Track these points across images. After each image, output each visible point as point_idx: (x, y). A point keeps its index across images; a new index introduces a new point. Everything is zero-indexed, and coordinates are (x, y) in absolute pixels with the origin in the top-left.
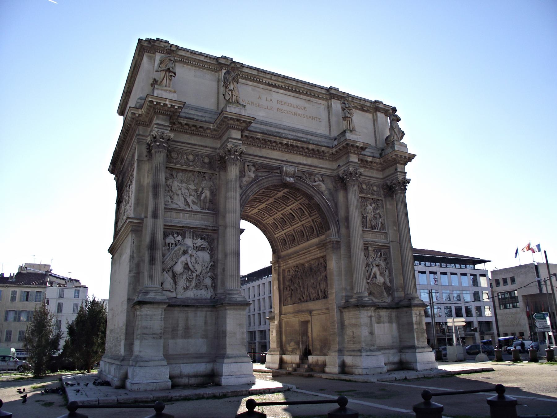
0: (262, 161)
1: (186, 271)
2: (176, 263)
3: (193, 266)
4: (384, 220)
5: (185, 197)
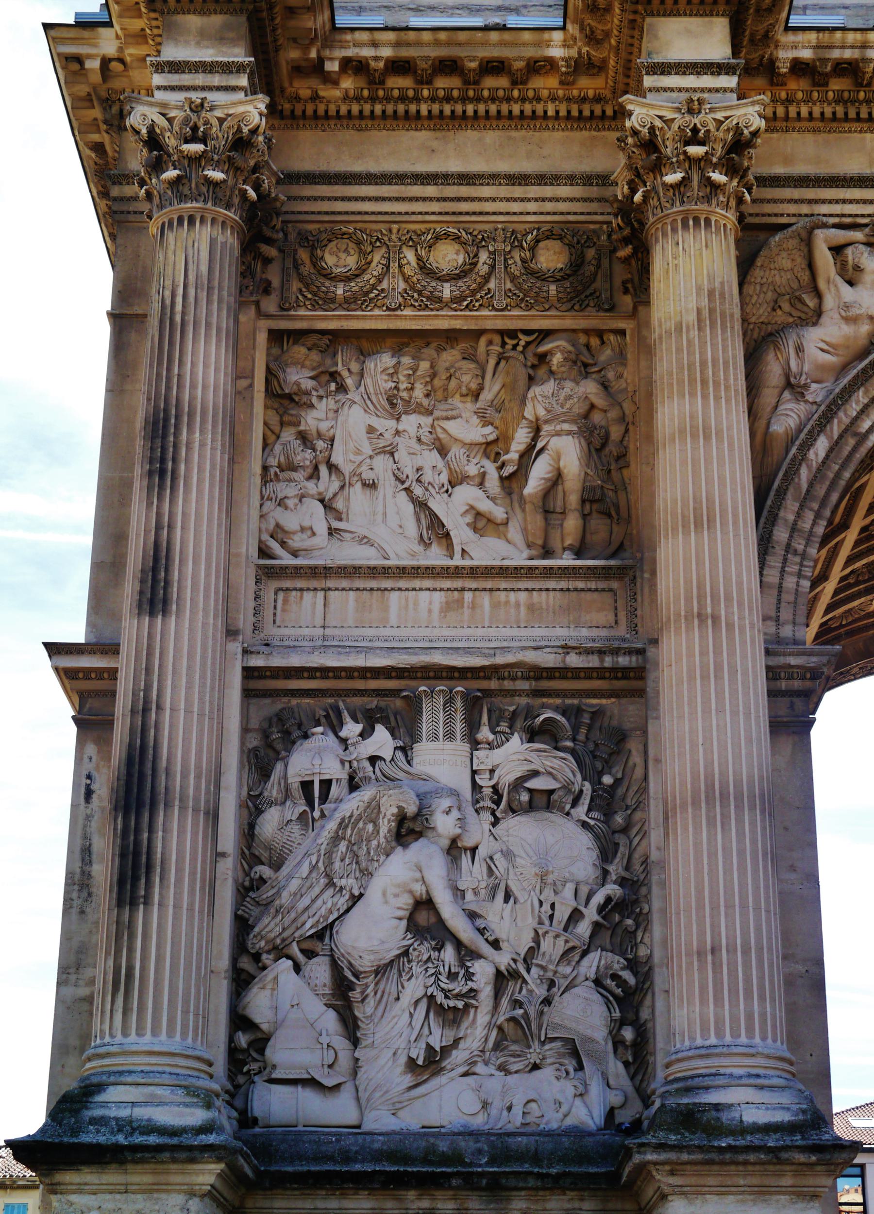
1: (424, 950)
2: (356, 899)
3: (472, 916)
5: (418, 491)
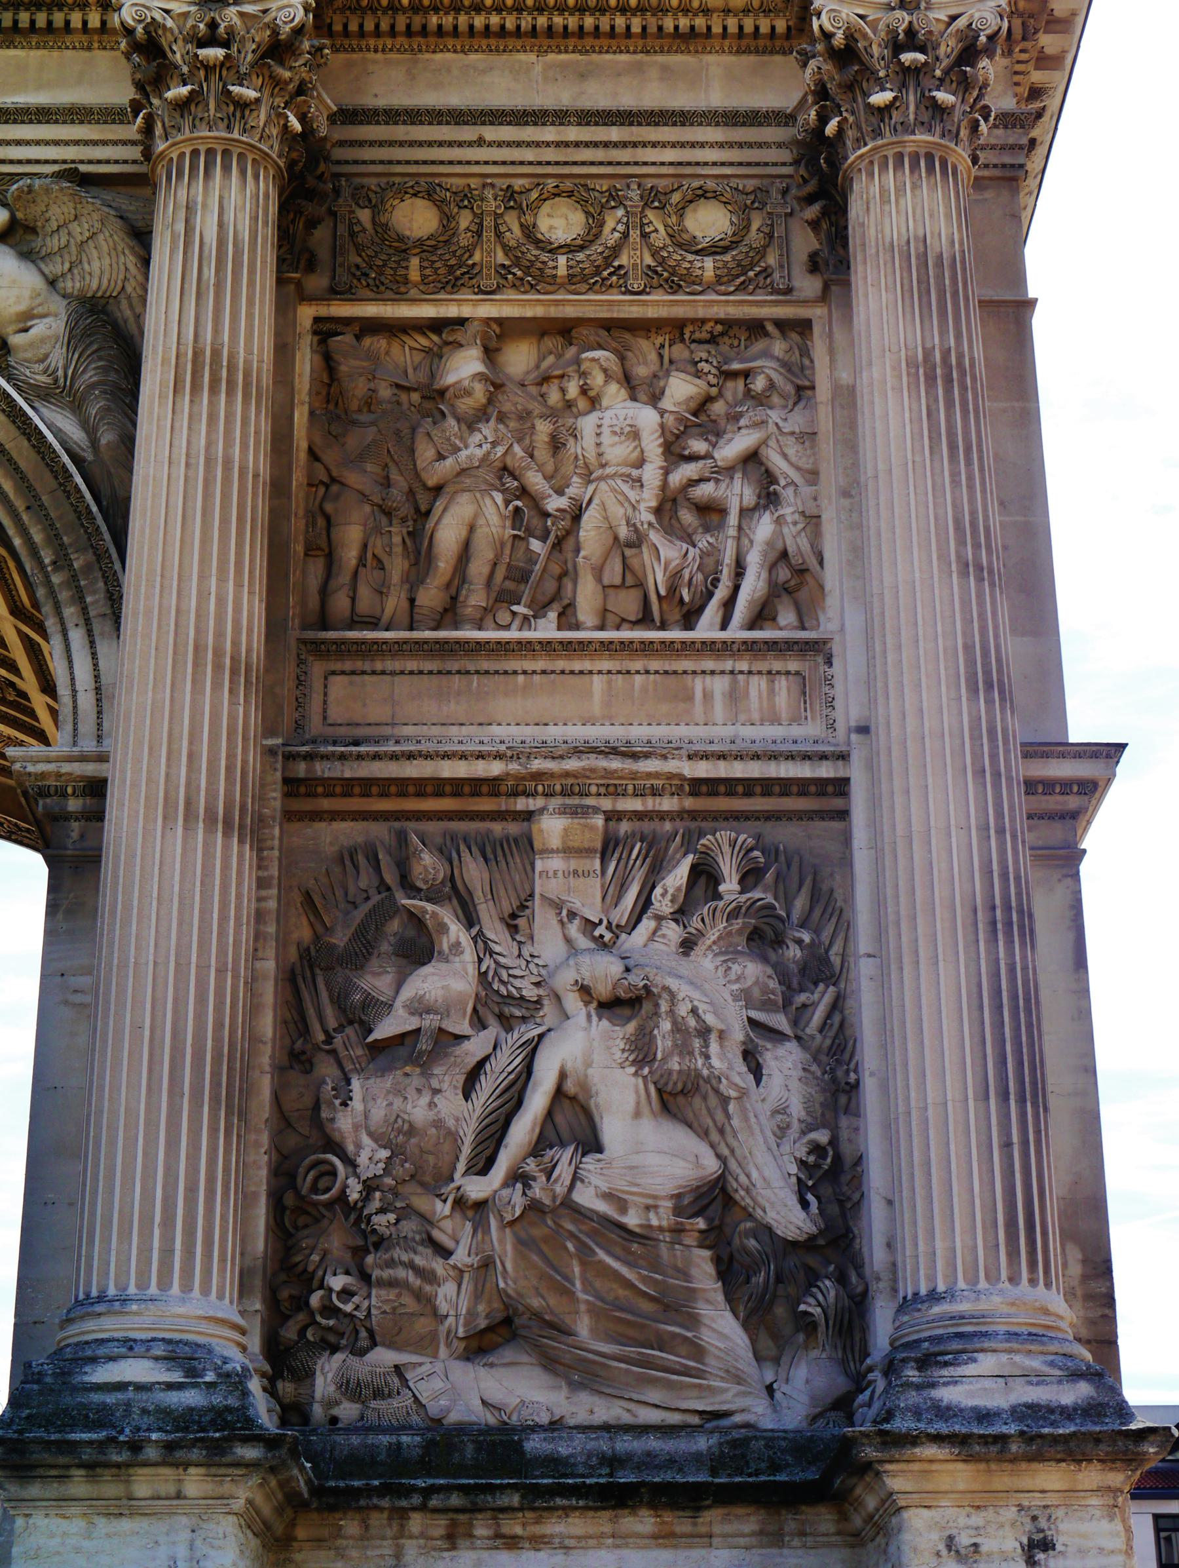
4: (813, 521)
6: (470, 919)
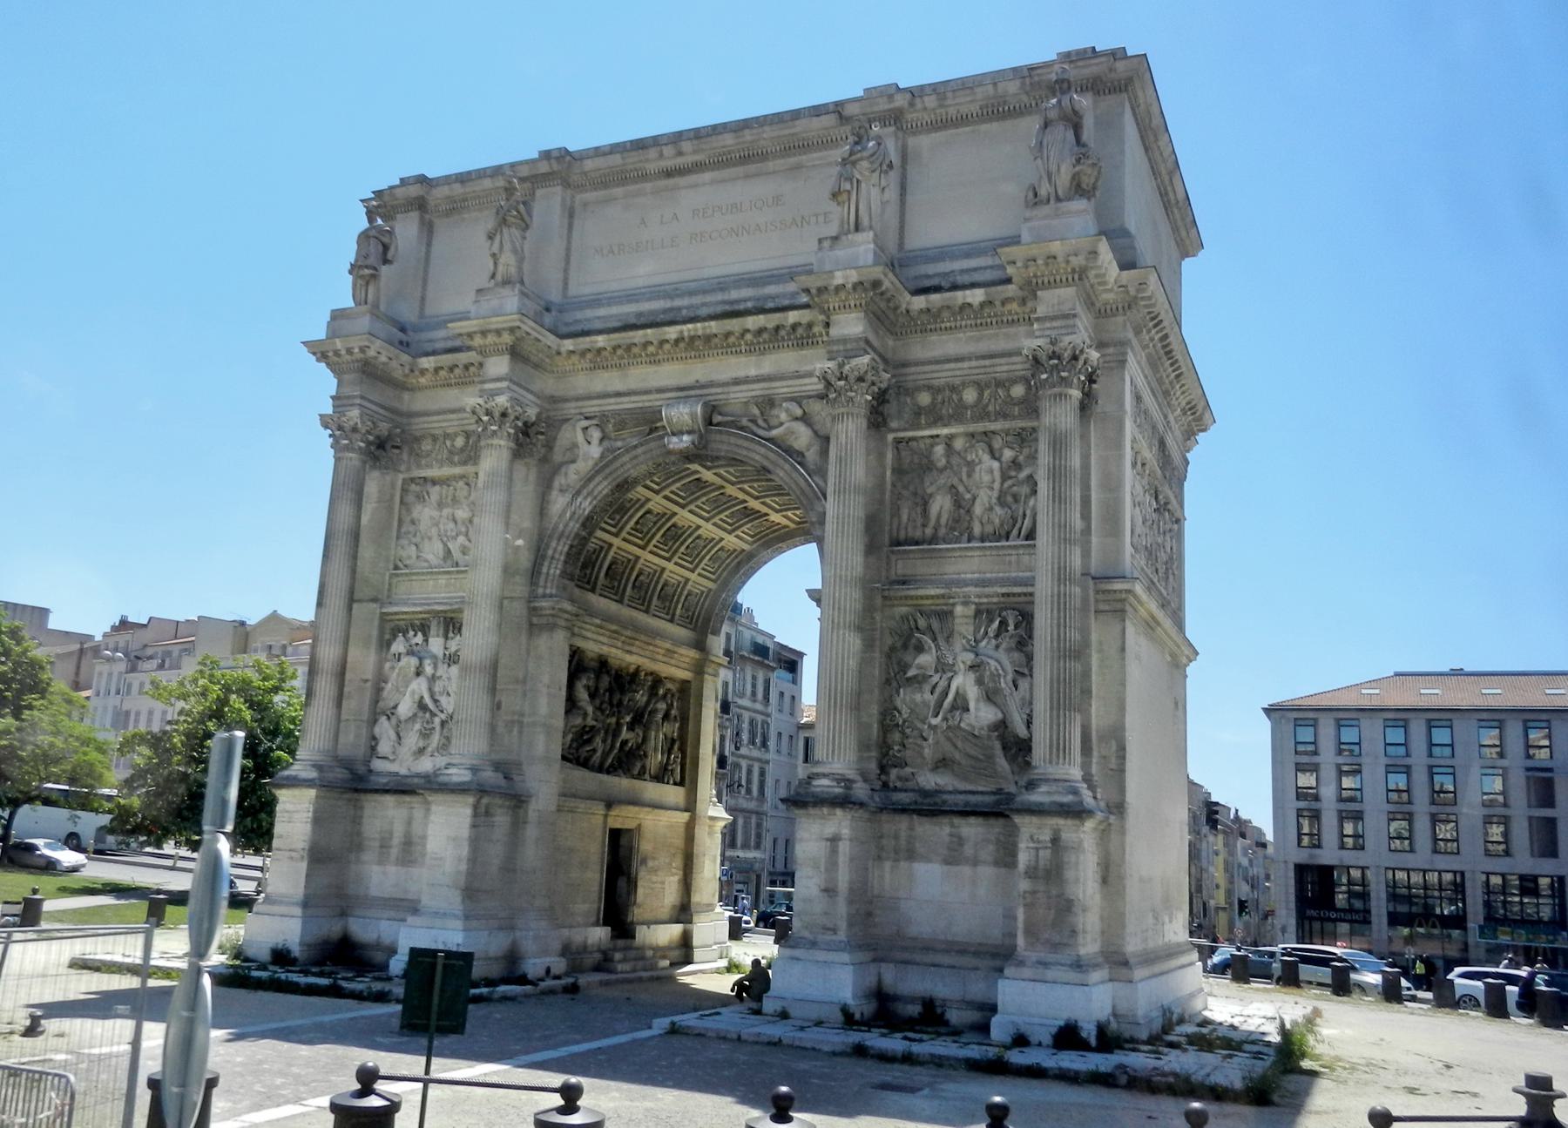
0: (627, 403)
1: (420, 714)
3: (436, 701)
6: (934, 640)
